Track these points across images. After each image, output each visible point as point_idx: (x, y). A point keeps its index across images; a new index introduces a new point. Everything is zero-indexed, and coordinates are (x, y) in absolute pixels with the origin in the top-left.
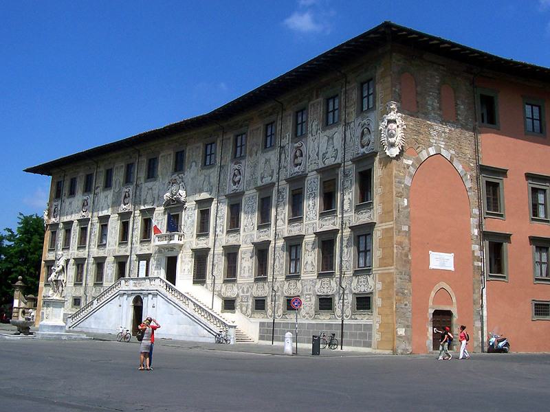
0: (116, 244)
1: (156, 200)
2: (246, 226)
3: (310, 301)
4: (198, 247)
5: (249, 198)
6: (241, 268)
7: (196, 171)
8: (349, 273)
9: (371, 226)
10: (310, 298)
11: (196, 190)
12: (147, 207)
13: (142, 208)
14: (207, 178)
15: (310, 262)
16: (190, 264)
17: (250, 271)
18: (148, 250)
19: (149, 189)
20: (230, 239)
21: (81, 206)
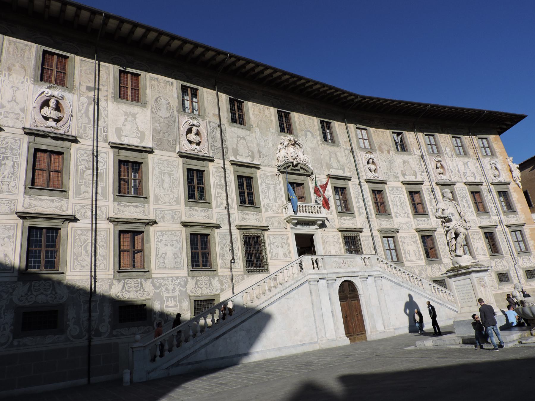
0: (177, 202)
1: (256, 156)
2: (397, 213)
3: (491, 276)
4: (344, 226)
5: (393, 189)
6: (405, 253)
7: (315, 142)
8: (515, 254)
9: (523, 225)
10: (490, 274)
11: (321, 163)
12: (240, 159)
13: (233, 158)
14: (333, 155)
15: (480, 248)
16: (338, 246)
17: (417, 255)
18: (259, 220)
19: (238, 137)
20: (383, 223)
21: (38, 106)
